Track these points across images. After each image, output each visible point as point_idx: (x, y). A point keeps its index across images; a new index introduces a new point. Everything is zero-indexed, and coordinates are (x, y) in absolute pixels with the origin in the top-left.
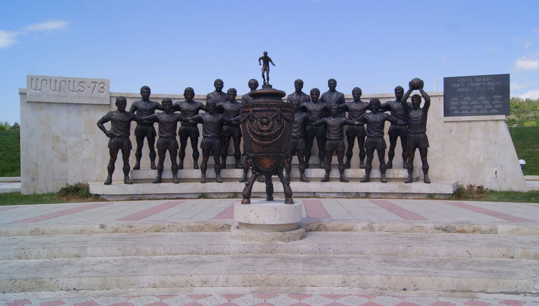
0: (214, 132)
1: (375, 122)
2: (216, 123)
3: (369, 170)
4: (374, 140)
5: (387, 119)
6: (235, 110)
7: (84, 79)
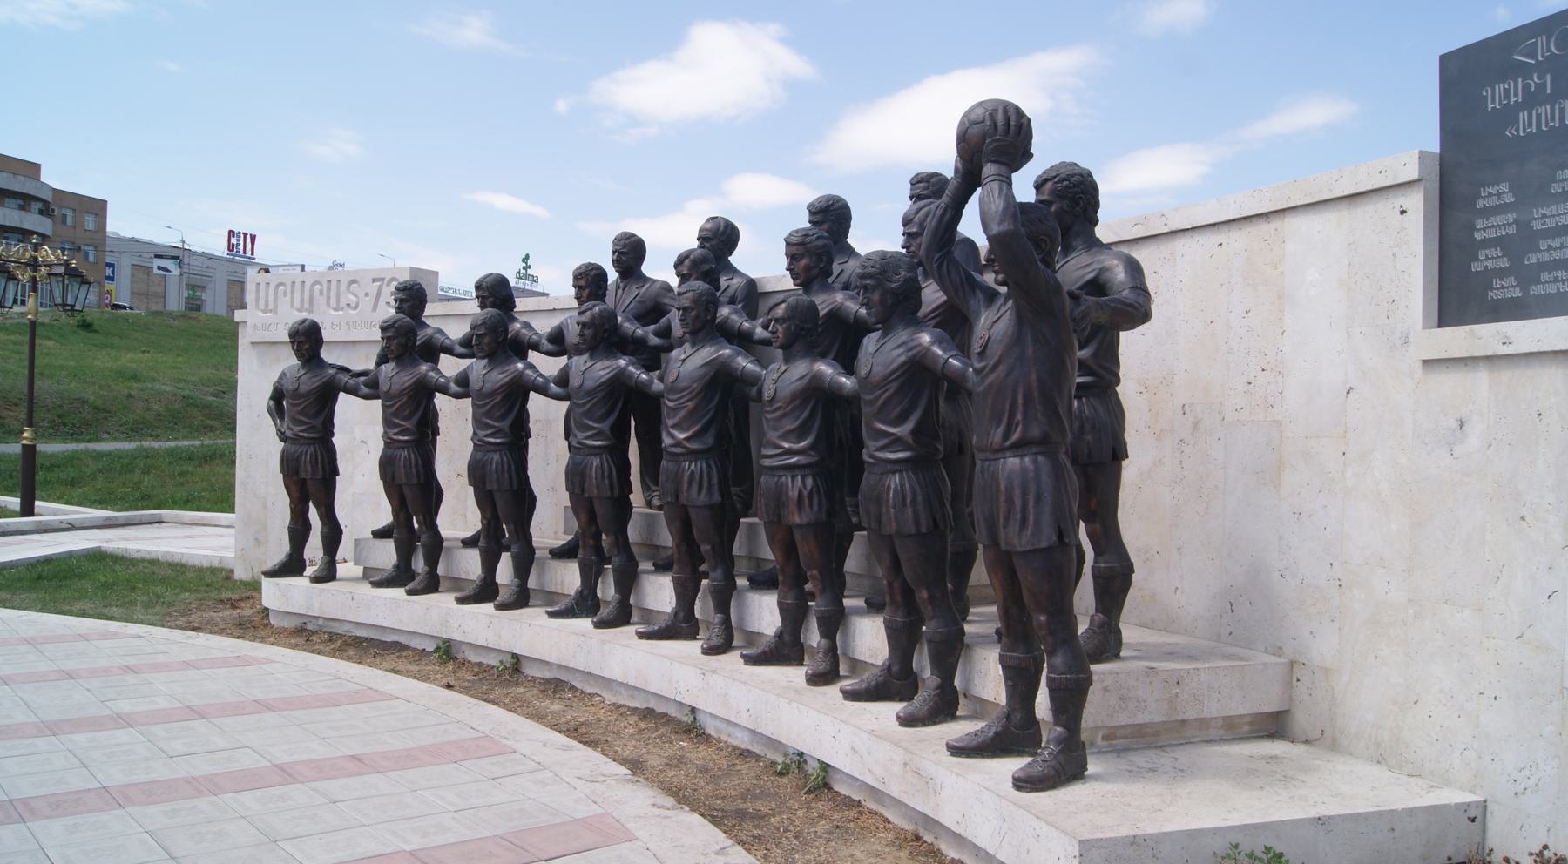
7: (357, 271)
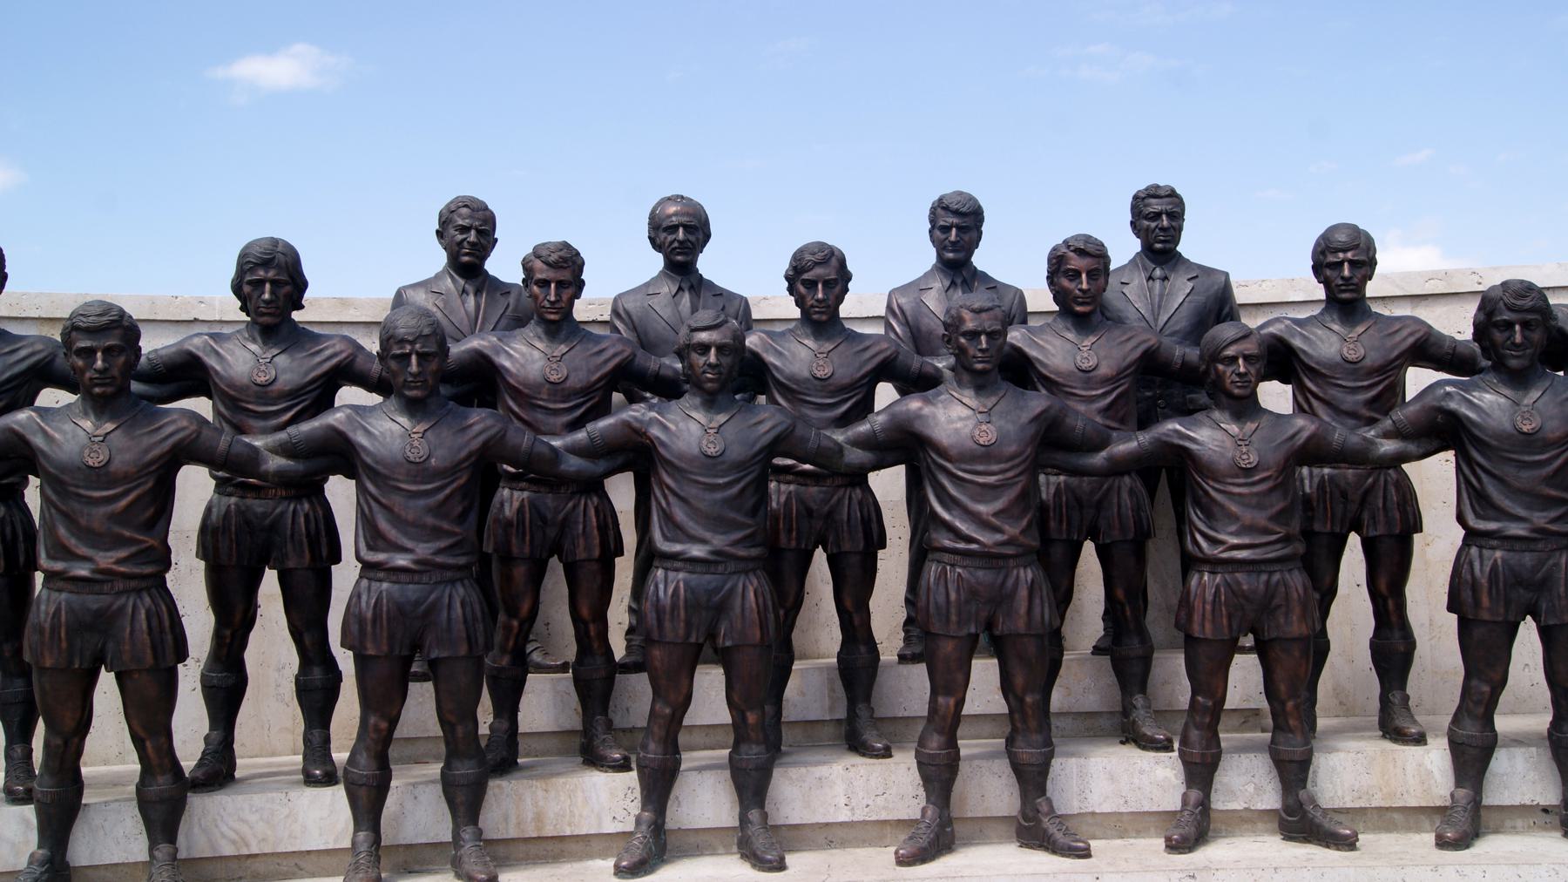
0: (437, 533)
2: (450, 471)
6: (576, 381)
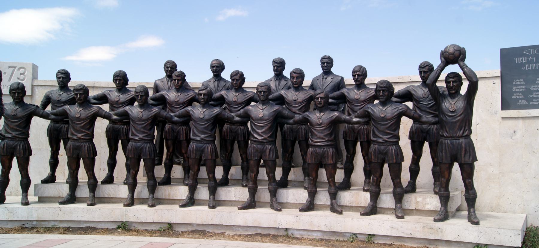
0: (144, 133)
1: (384, 119)
2: (147, 120)
3: (375, 196)
4: (382, 147)
5: (406, 113)
